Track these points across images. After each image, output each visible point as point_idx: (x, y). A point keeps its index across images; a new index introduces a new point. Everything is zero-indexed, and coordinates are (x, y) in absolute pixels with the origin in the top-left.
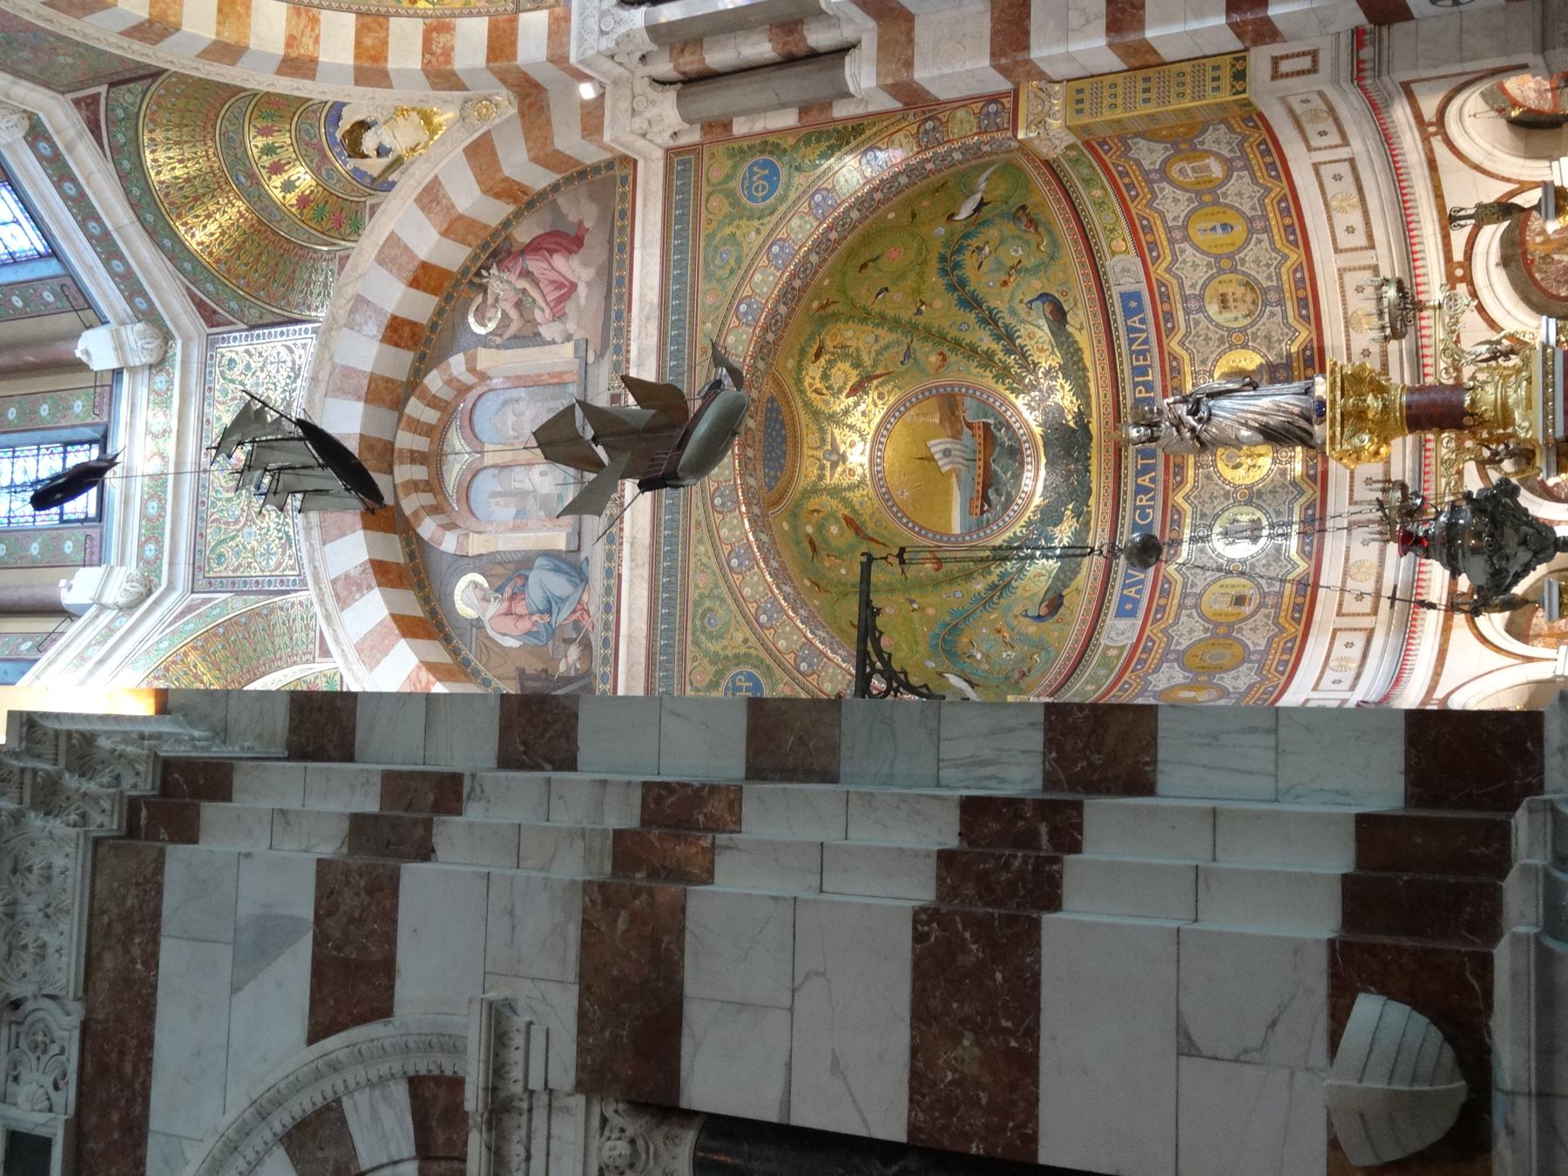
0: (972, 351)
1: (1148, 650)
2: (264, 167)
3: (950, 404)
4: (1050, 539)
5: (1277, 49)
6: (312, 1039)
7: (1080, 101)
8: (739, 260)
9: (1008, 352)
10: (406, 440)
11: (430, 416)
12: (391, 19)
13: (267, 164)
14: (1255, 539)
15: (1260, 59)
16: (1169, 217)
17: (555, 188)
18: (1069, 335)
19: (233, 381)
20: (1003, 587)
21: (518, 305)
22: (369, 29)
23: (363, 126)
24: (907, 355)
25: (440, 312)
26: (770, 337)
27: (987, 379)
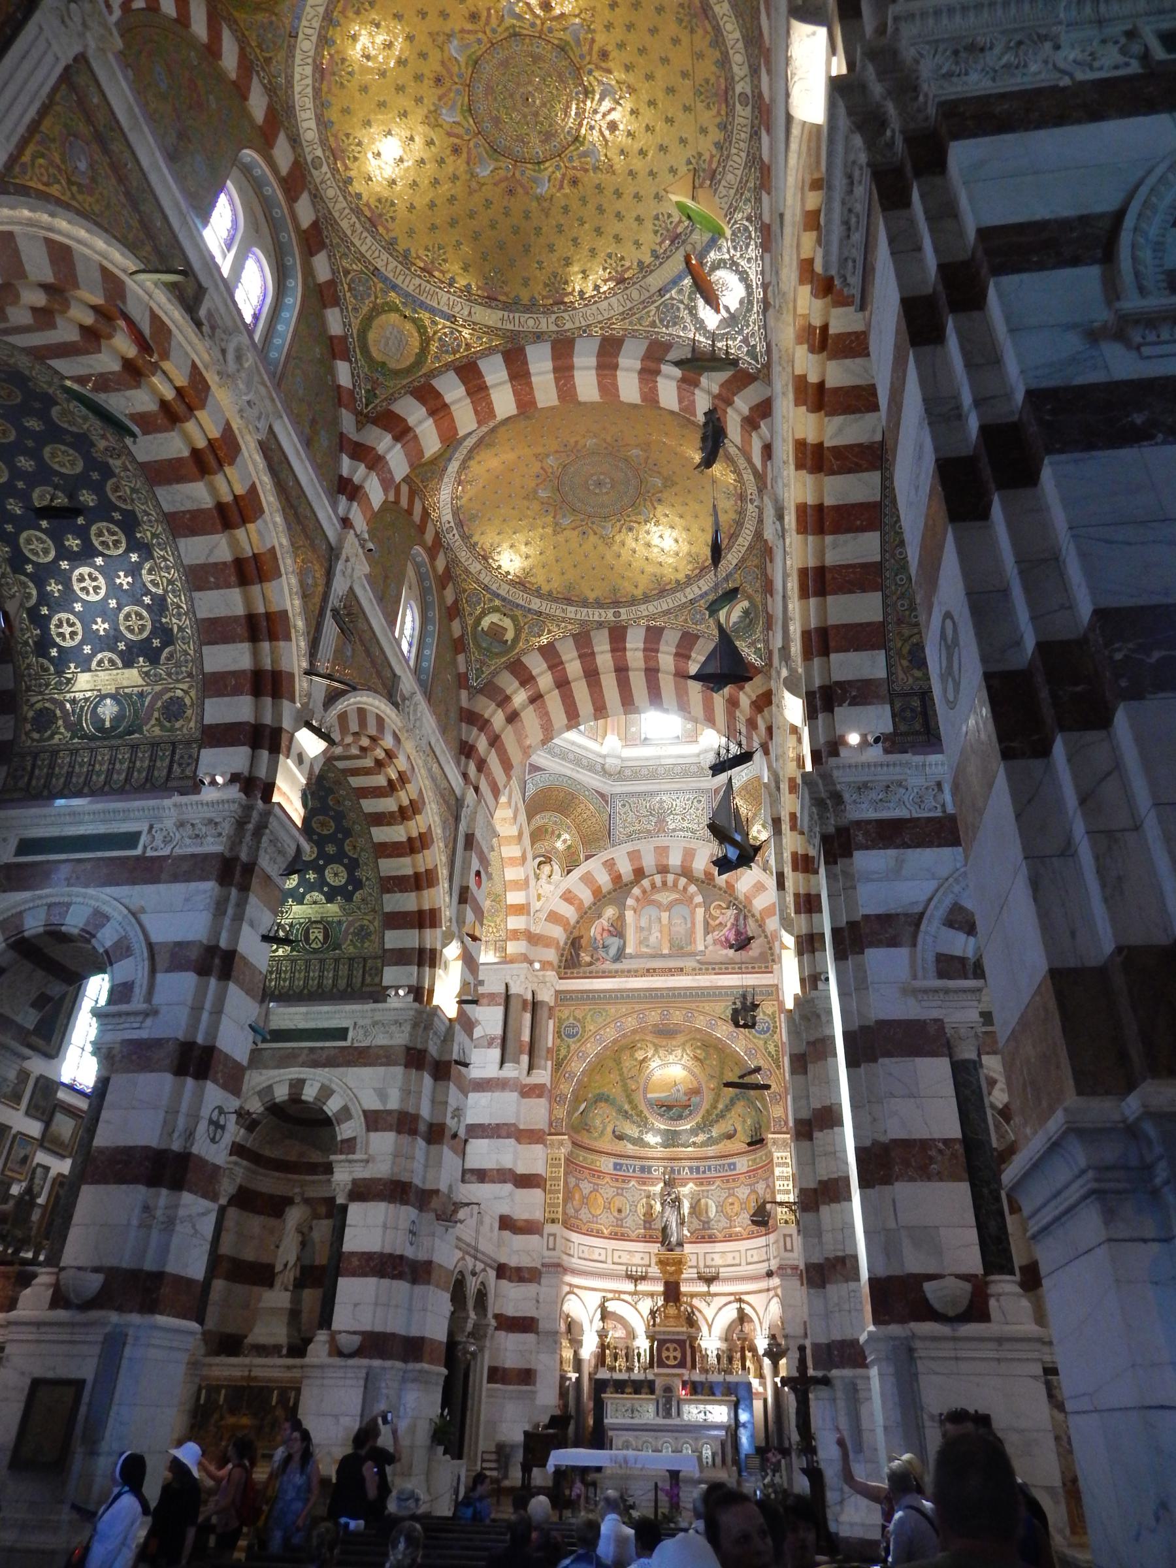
0: (716, 1101)
3: (696, 1092)
6: (364, 1112)
10: (670, 878)
11: (681, 887)
20: (626, 1116)
27: (706, 1106)
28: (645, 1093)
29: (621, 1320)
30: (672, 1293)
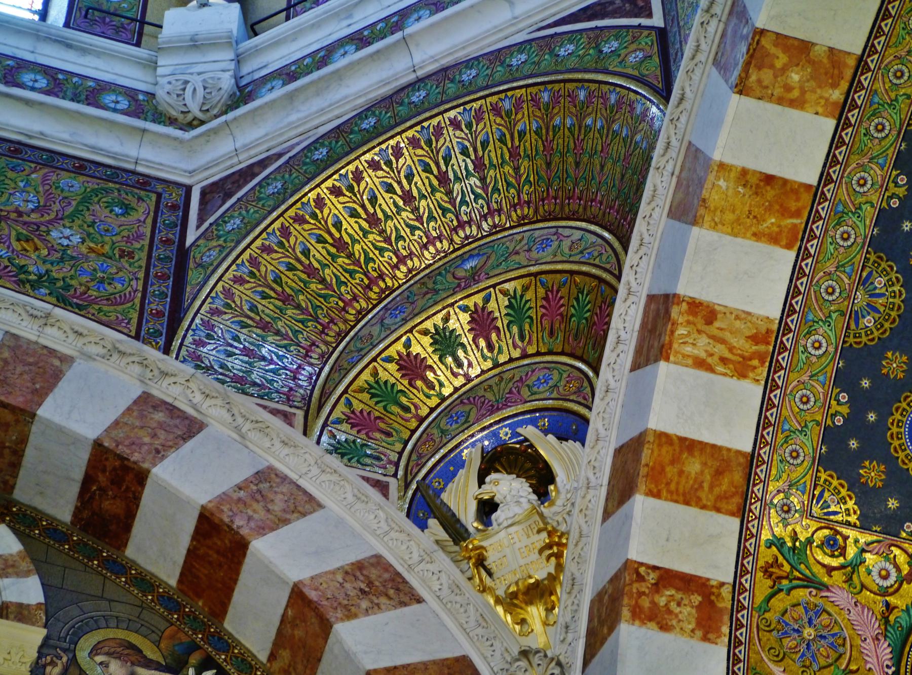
2: (487, 300)
12: (736, 522)
13: (492, 305)
19: (86, 200)
22: (718, 473)
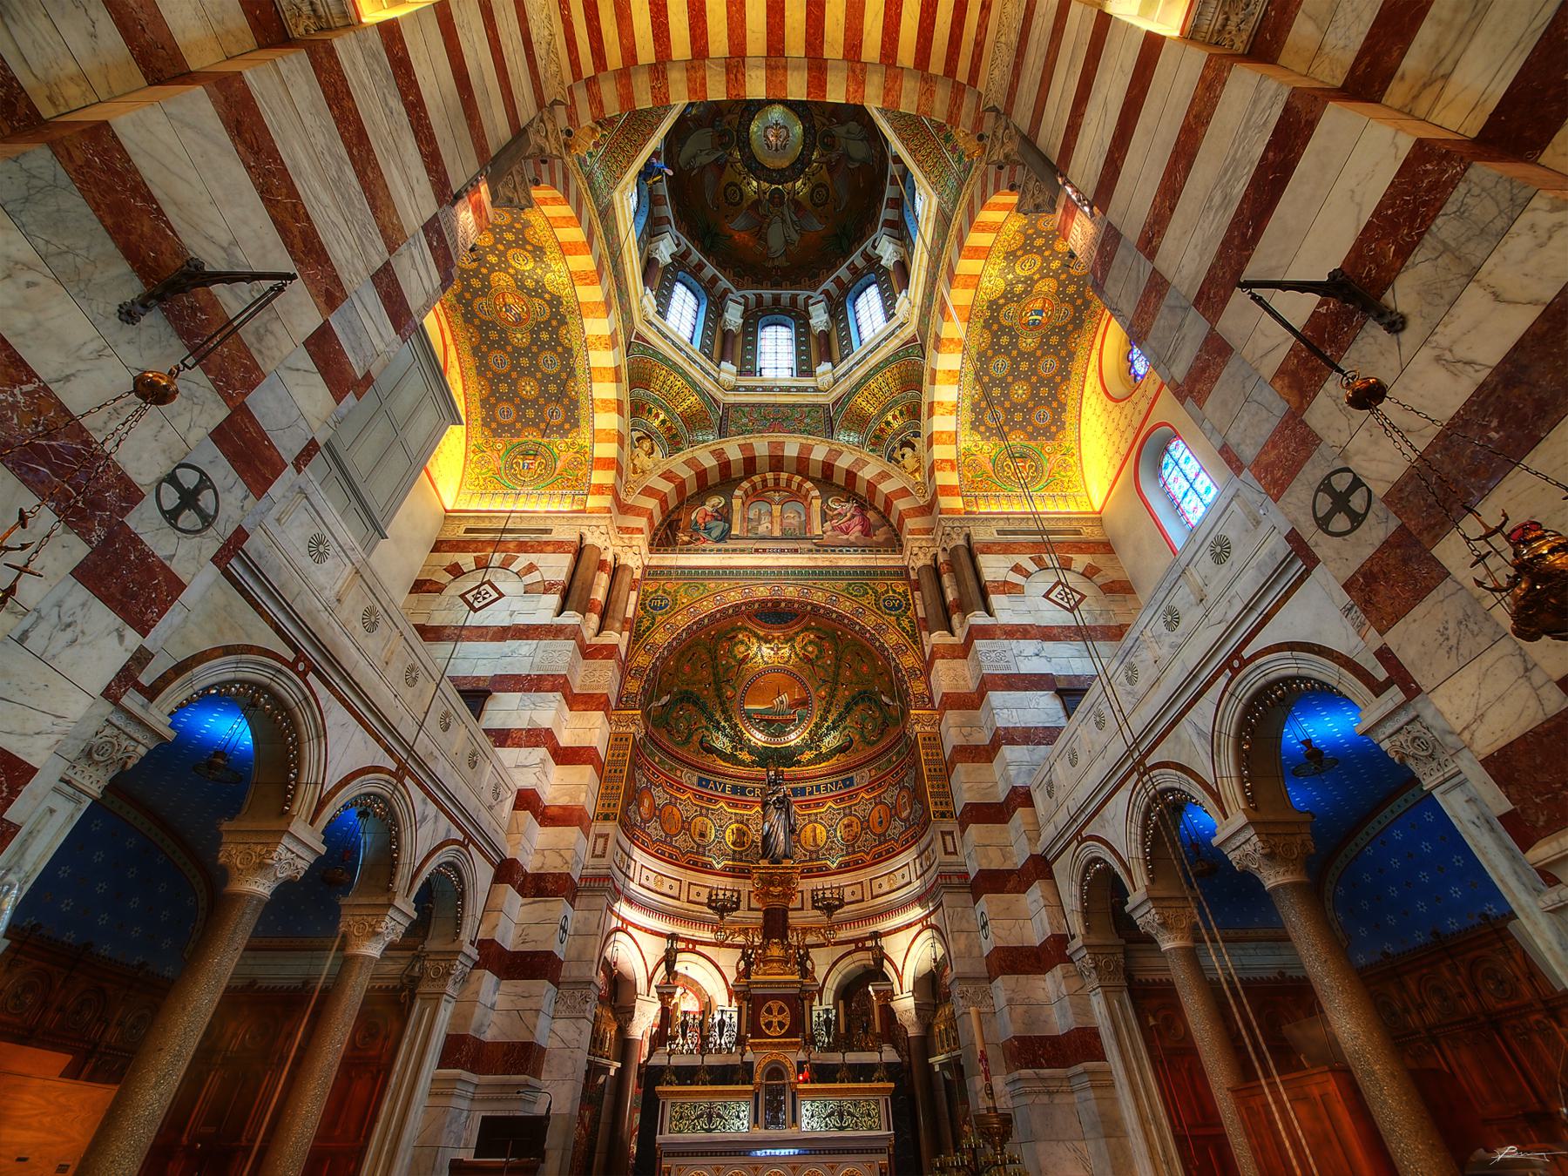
0: (827, 711)
1: (678, 790)
4: (741, 749)
5: (957, 834)
7: (929, 739)
8: (855, 596)
9: (827, 729)
10: (784, 475)
11: (794, 486)
14: (733, 844)
15: (951, 825)
16: (885, 795)
17: (891, 526)
18: (835, 755)
20: (718, 727)
21: (840, 514)
23: (913, 448)
24: (824, 681)
25: (838, 486)
26: (822, 611)
28: (743, 701)
29: (693, 986)
30: (775, 924)
